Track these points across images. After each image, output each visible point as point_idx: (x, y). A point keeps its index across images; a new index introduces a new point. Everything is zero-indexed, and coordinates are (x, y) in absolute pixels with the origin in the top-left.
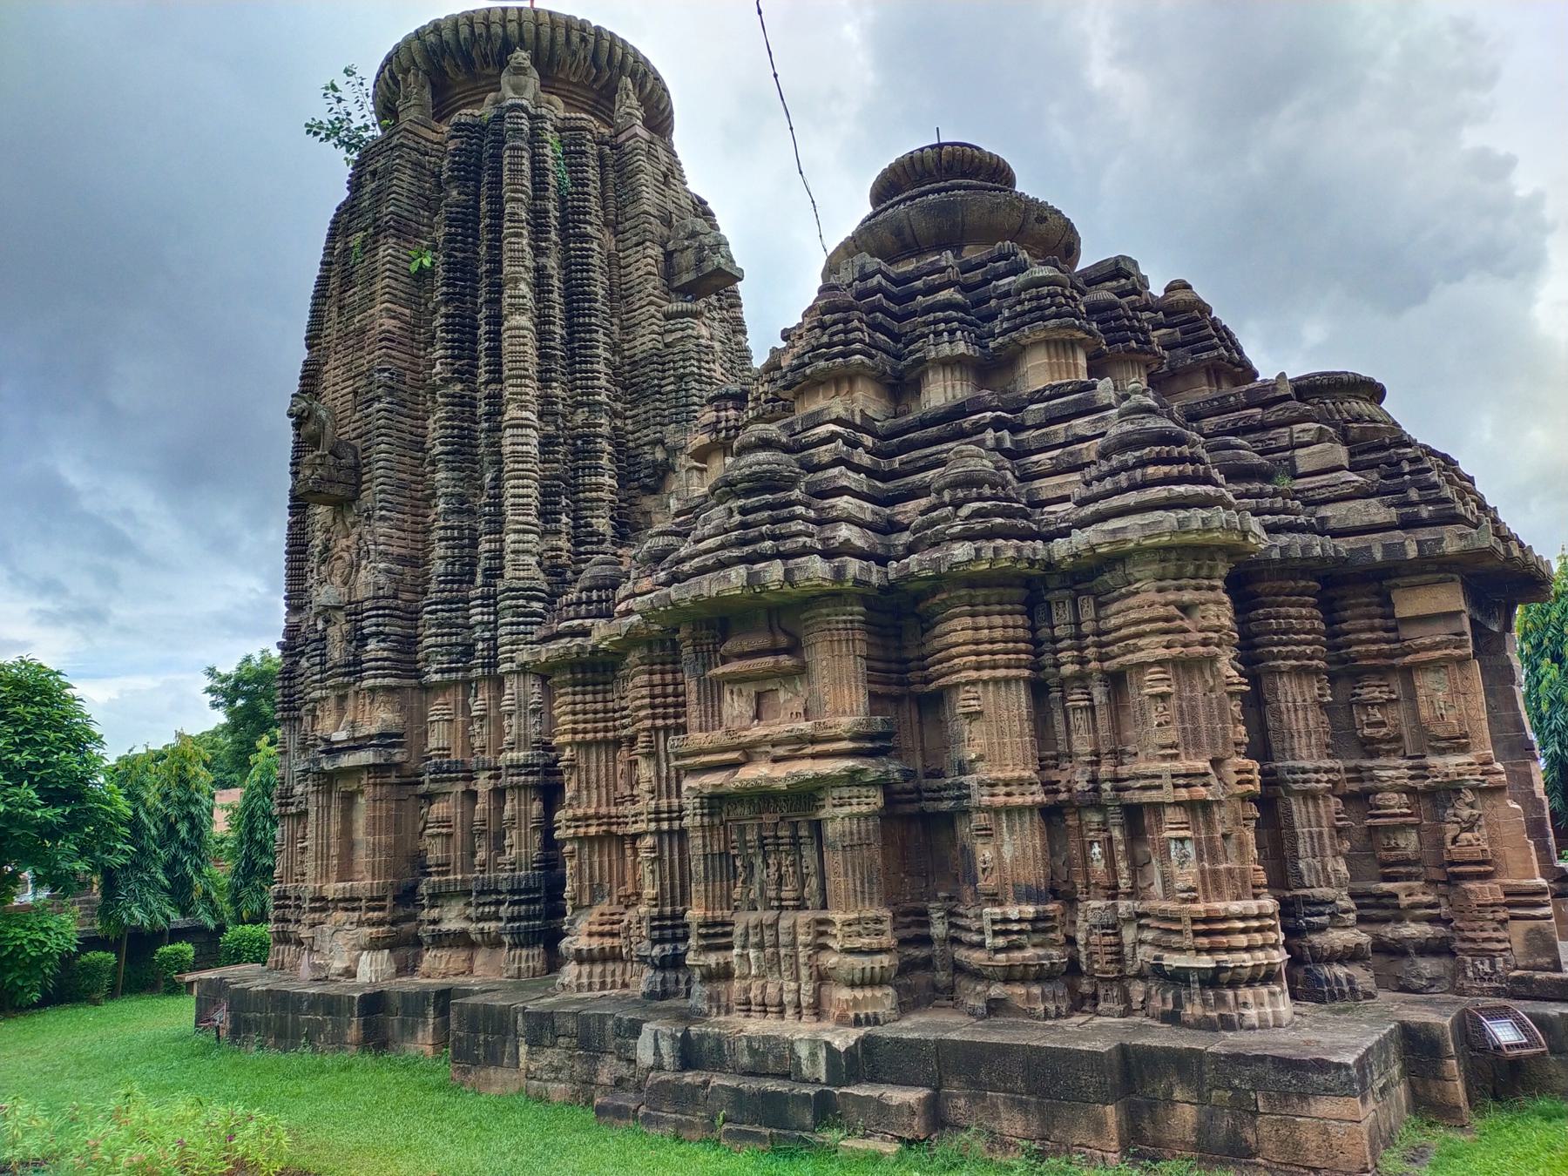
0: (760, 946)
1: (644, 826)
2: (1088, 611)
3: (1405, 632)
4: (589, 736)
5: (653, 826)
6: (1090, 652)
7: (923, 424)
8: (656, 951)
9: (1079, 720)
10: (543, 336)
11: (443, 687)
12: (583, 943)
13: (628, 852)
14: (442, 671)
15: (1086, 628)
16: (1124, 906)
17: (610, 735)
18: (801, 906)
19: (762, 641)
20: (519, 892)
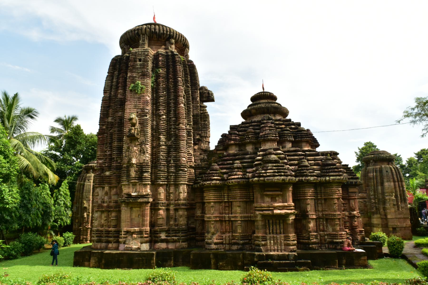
0: (273, 240)
1: (239, 219)
2: (323, 188)
3: (349, 194)
4: (217, 201)
5: (241, 219)
6: (323, 195)
7: (288, 151)
8: (241, 242)
9: (320, 205)
10: (185, 108)
11: (162, 185)
12: (215, 241)
13: (224, 223)
14: (162, 181)
15: (323, 191)
16: (325, 233)
17: (220, 200)
18: (280, 233)
19: (277, 189)
20: (184, 231)
